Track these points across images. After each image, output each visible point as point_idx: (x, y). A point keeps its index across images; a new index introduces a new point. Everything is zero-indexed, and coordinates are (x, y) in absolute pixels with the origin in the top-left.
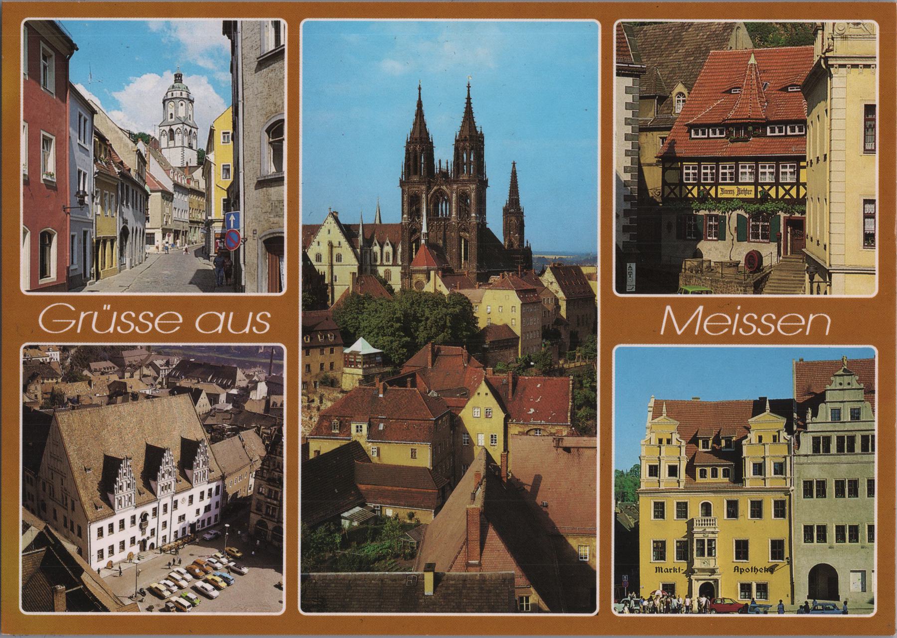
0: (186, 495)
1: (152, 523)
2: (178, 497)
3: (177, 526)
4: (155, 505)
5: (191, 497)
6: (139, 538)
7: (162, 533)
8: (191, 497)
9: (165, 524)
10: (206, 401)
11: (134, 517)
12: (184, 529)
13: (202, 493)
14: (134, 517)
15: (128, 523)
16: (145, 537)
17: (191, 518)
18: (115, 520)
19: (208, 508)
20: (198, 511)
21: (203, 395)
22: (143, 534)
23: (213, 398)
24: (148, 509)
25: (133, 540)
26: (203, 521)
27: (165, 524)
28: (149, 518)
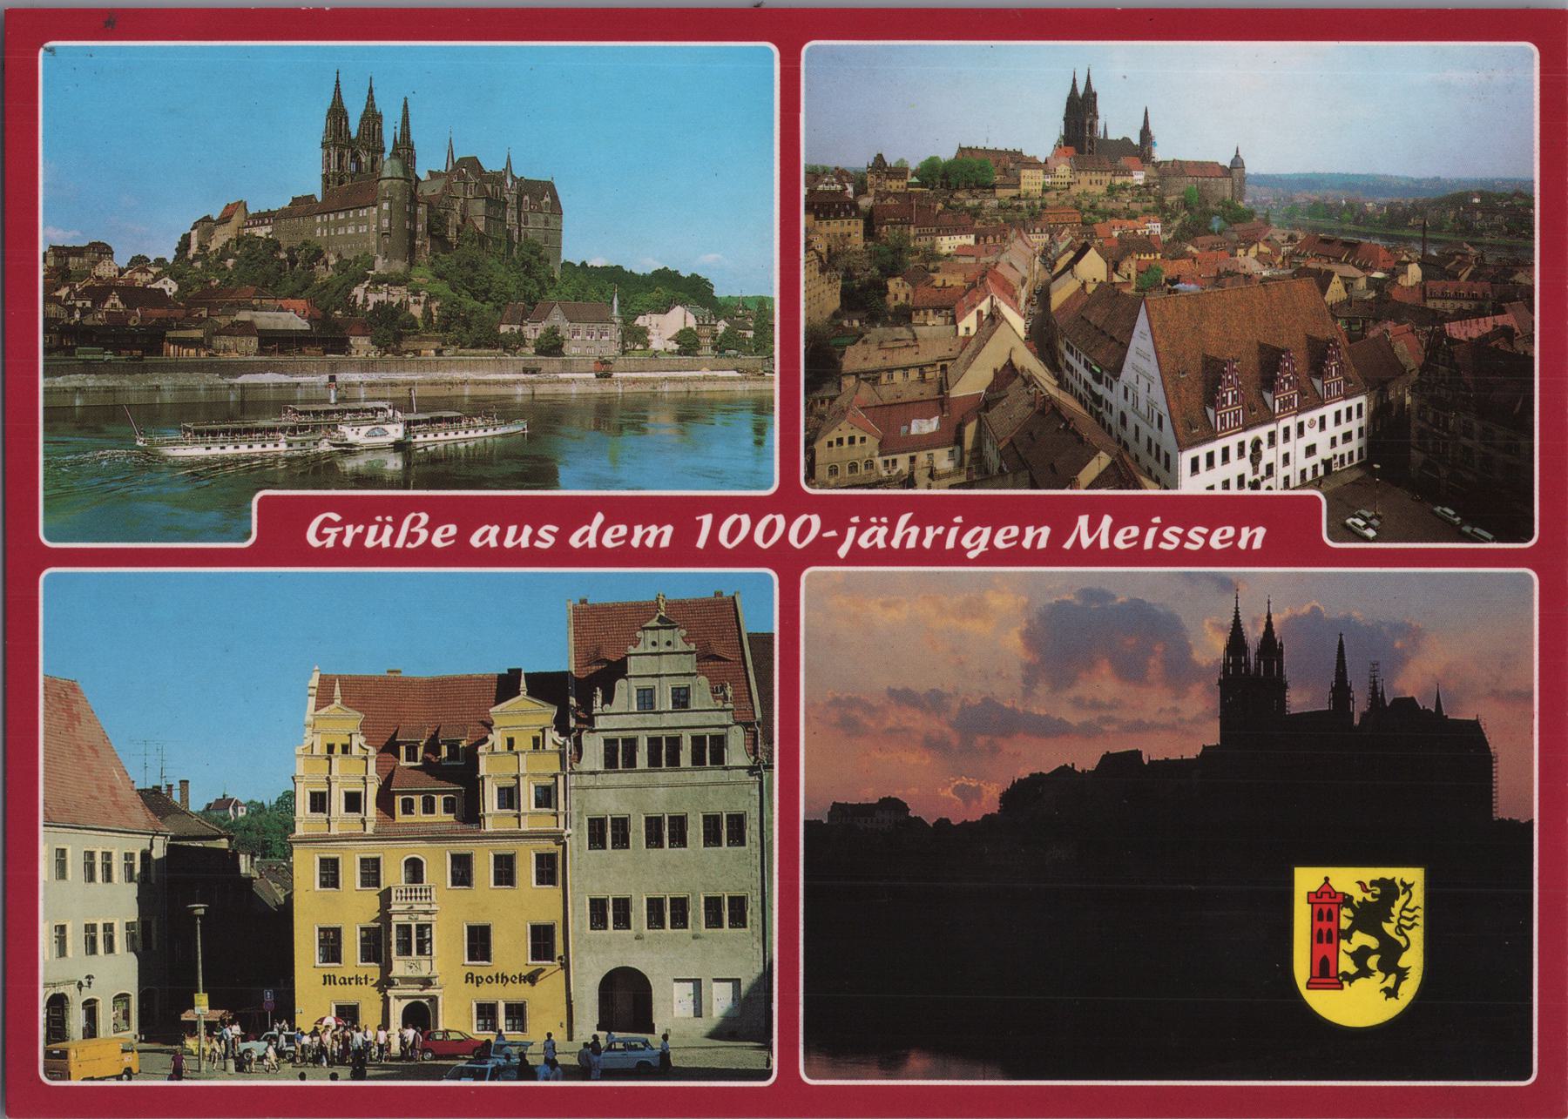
0: (1315, 414)
1: (1269, 455)
2: (1305, 418)
3: (1301, 462)
4: (1272, 427)
5: (1322, 419)
6: (1249, 478)
7: (1281, 472)
8: (1322, 419)
9: (1286, 458)
10: (1341, 286)
11: (1242, 445)
12: (1315, 467)
13: (1338, 414)
14: (1242, 445)
15: (1233, 453)
16: (1258, 477)
17: (1324, 452)
18: (1216, 447)
19: (1347, 437)
20: (1333, 442)
21: (1336, 279)
22: (1256, 471)
23: (1348, 283)
24: (1262, 432)
25: (1241, 479)
26: (1342, 456)
27: (1286, 458)
28: (1264, 447)
